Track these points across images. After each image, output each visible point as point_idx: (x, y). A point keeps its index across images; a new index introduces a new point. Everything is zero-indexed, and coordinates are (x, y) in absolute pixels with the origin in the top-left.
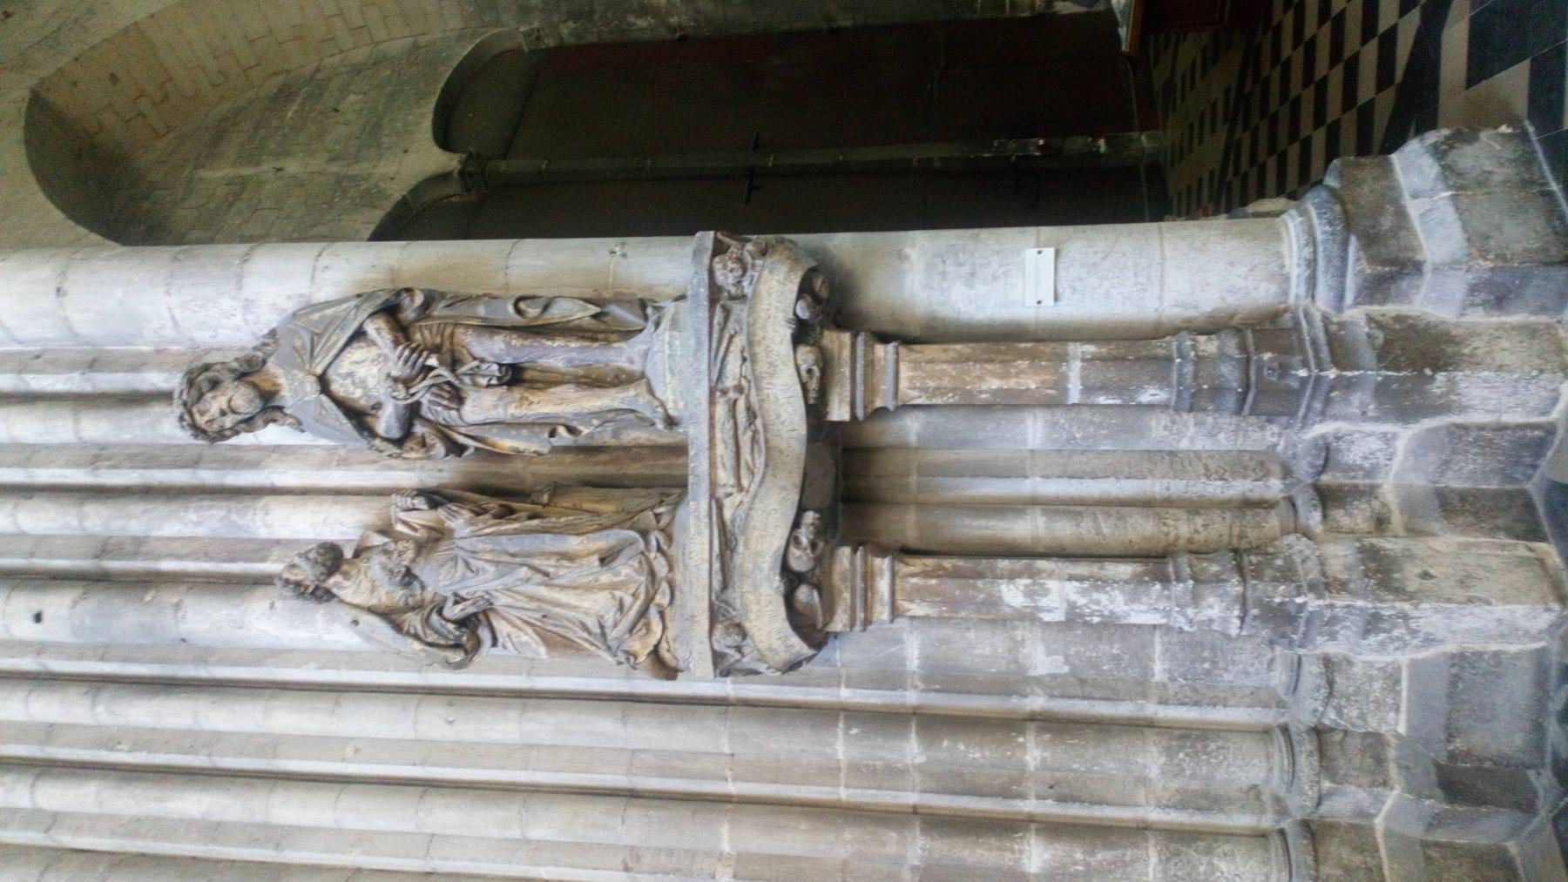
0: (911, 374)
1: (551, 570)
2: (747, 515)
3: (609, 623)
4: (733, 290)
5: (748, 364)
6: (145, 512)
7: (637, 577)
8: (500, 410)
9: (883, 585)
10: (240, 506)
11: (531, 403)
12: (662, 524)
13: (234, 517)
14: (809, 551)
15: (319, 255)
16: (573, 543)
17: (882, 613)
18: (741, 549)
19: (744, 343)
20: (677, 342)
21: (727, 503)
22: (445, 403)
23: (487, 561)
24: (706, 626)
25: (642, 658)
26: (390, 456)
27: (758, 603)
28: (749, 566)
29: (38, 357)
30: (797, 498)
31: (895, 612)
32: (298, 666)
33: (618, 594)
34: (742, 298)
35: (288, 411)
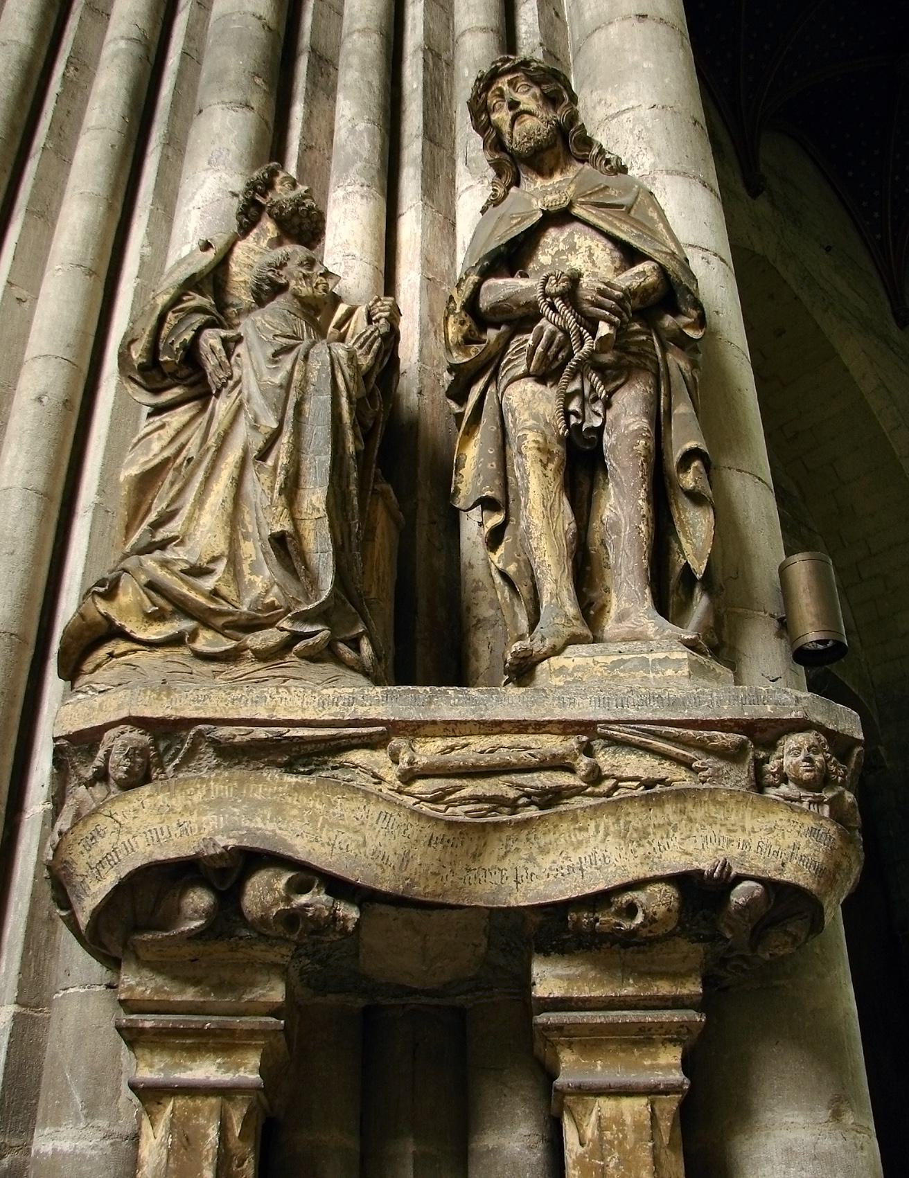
0: (629, 1120)
1: (270, 463)
2: (356, 790)
3: (169, 555)
4: (771, 766)
5: (640, 791)
6: (370, 83)
7: (247, 600)
8: (530, 423)
9: (205, 1070)
10: (374, 173)
11: (545, 466)
12: (345, 651)
13: (359, 164)
14: (282, 906)
15: (722, 260)
16: (315, 496)
17: (151, 1070)
18: (291, 779)
19: (677, 785)
20: (670, 672)
21: (381, 756)
22: (540, 349)
23: (291, 374)
24: (148, 713)
25: (102, 606)
26: (451, 298)
27: (185, 807)
28: (259, 792)
29: (557, 15)
30: (385, 887)
31: (151, 1095)
32: (148, 234)
33: (221, 567)
34: (759, 784)
35: (513, 190)
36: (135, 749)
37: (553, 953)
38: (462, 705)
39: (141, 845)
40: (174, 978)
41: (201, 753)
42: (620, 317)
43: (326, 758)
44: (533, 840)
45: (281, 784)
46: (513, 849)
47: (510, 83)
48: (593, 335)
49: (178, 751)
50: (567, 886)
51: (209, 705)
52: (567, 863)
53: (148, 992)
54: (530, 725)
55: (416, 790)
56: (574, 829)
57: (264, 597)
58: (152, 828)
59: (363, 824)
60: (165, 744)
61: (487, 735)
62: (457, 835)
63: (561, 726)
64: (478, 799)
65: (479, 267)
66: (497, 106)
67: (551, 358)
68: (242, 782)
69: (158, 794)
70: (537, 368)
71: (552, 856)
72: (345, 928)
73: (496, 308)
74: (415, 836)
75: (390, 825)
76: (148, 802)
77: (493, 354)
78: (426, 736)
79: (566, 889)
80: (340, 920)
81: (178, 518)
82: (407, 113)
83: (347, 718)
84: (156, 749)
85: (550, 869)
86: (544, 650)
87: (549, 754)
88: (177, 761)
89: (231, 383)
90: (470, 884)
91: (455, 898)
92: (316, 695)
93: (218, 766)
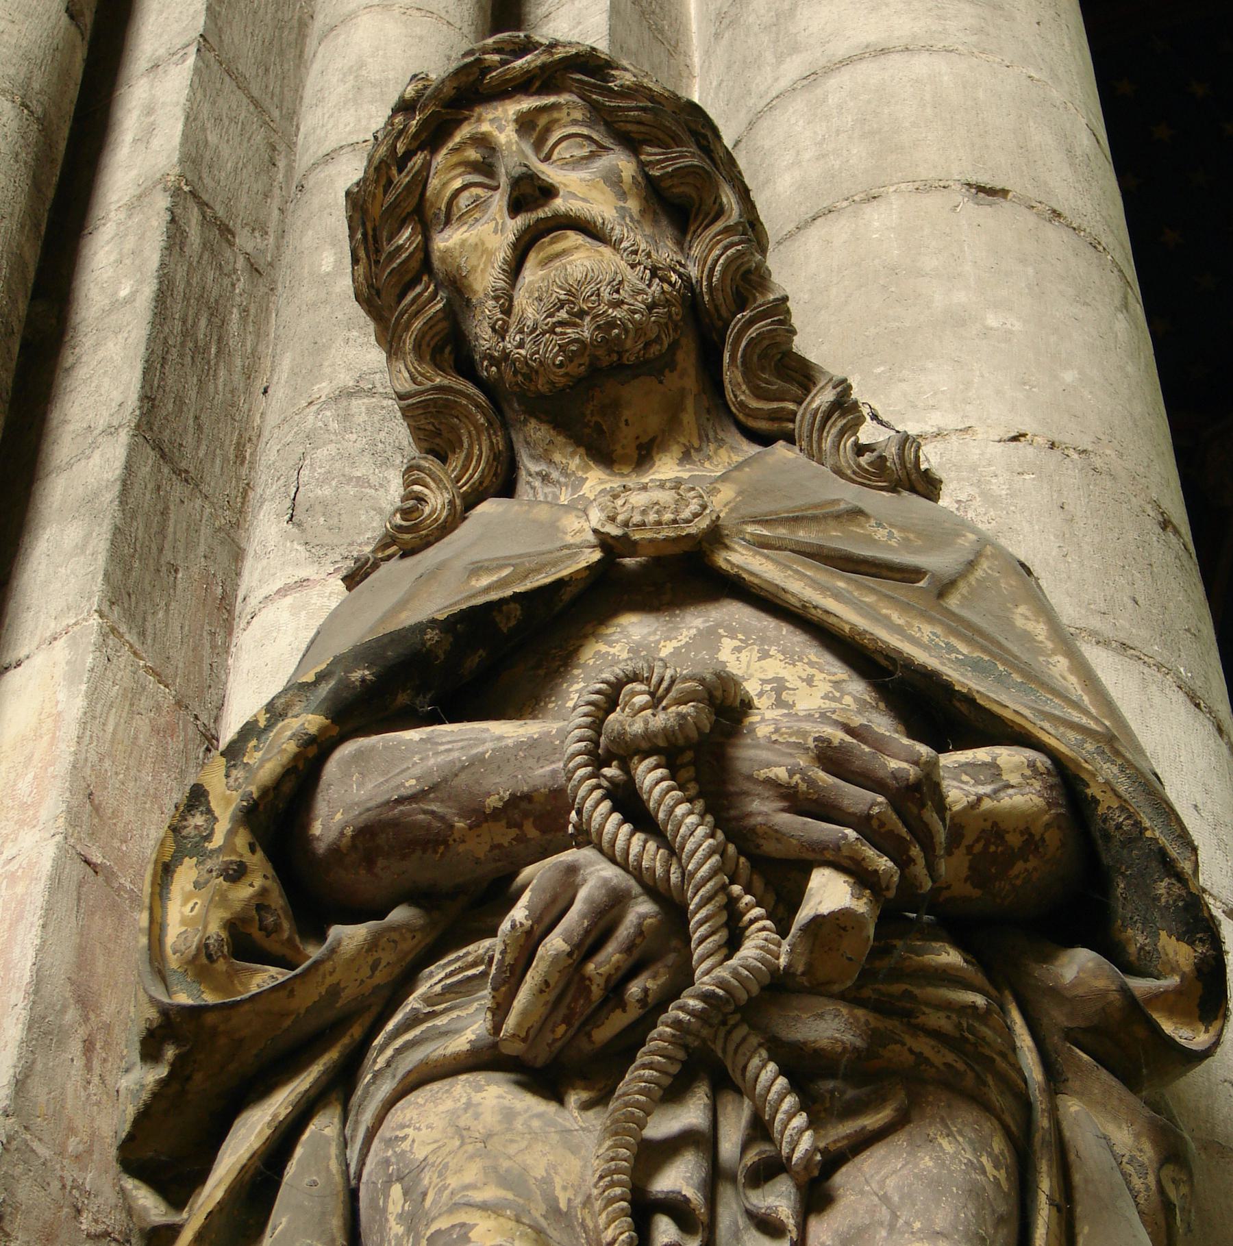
22: (555, 943)
26: (197, 797)
35: (490, 508)
42: (903, 862)
47: (525, 124)
48: (782, 917)
65: (325, 689)
66: (464, 200)
67: (596, 992)
70: (534, 1019)
77: (349, 994)
82: (82, 372)
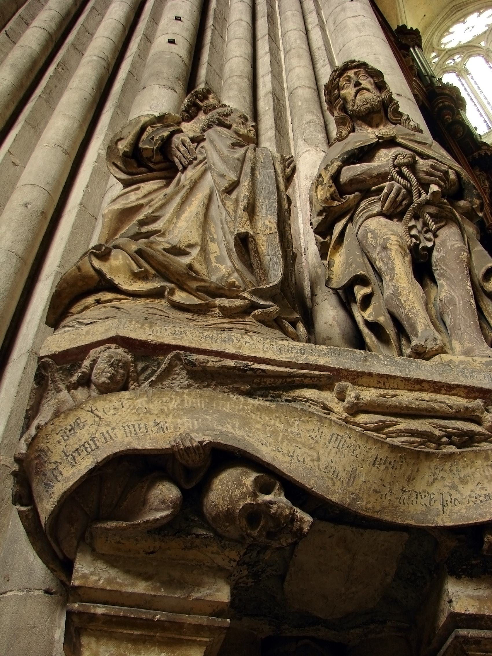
1: (234, 196)
6: (244, 98)
12: (287, 324)
14: (249, 500)
22: (392, 195)
24: (133, 336)
27: (162, 411)
28: (227, 408)
35: (351, 134)
36: (119, 361)
37: (463, 576)
38: (389, 365)
39: (119, 437)
40: (127, 572)
41: (175, 374)
42: (445, 184)
43: (281, 392)
44: (455, 471)
45: (247, 405)
46: (439, 477)
47: (355, 73)
49: (154, 372)
50: (485, 510)
51: (185, 338)
52: (483, 492)
53: (101, 582)
54: (443, 387)
55: (361, 421)
56: (487, 465)
57: (228, 278)
58: (130, 424)
59: (317, 442)
60: (143, 365)
61: (410, 390)
62: (398, 459)
63: (466, 391)
64: (413, 433)
65: (340, 158)
67: (398, 203)
68: (212, 399)
69: (137, 399)
70: (389, 207)
71: (470, 486)
72: (301, 529)
73: (353, 181)
74: (362, 456)
75: (341, 446)
76: (127, 404)
77: (351, 205)
78: (362, 386)
79: (486, 513)
80: (297, 521)
81: (159, 222)
82: (262, 121)
83: (300, 362)
84: (136, 367)
85: (470, 496)
86: (436, 347)
87: (462, 406)
88: (153, 378)
89: (195, 162)
90: (404, 504)
91: (391, 515)
92: (274, 344)
93: (189, 386)
